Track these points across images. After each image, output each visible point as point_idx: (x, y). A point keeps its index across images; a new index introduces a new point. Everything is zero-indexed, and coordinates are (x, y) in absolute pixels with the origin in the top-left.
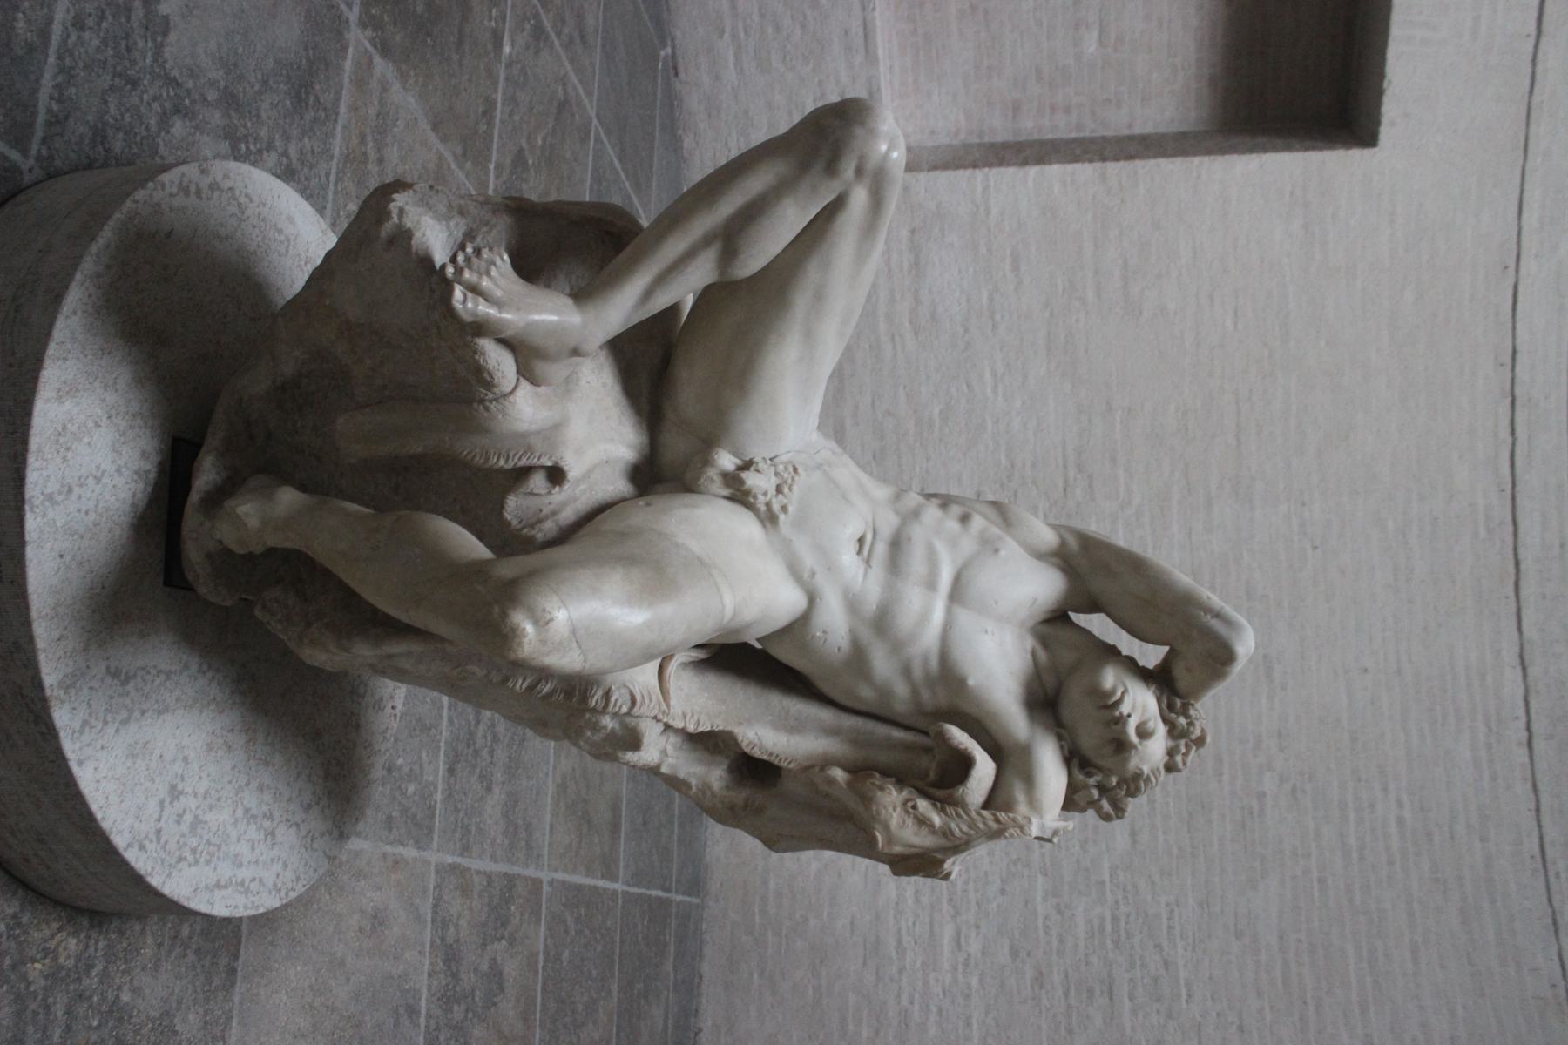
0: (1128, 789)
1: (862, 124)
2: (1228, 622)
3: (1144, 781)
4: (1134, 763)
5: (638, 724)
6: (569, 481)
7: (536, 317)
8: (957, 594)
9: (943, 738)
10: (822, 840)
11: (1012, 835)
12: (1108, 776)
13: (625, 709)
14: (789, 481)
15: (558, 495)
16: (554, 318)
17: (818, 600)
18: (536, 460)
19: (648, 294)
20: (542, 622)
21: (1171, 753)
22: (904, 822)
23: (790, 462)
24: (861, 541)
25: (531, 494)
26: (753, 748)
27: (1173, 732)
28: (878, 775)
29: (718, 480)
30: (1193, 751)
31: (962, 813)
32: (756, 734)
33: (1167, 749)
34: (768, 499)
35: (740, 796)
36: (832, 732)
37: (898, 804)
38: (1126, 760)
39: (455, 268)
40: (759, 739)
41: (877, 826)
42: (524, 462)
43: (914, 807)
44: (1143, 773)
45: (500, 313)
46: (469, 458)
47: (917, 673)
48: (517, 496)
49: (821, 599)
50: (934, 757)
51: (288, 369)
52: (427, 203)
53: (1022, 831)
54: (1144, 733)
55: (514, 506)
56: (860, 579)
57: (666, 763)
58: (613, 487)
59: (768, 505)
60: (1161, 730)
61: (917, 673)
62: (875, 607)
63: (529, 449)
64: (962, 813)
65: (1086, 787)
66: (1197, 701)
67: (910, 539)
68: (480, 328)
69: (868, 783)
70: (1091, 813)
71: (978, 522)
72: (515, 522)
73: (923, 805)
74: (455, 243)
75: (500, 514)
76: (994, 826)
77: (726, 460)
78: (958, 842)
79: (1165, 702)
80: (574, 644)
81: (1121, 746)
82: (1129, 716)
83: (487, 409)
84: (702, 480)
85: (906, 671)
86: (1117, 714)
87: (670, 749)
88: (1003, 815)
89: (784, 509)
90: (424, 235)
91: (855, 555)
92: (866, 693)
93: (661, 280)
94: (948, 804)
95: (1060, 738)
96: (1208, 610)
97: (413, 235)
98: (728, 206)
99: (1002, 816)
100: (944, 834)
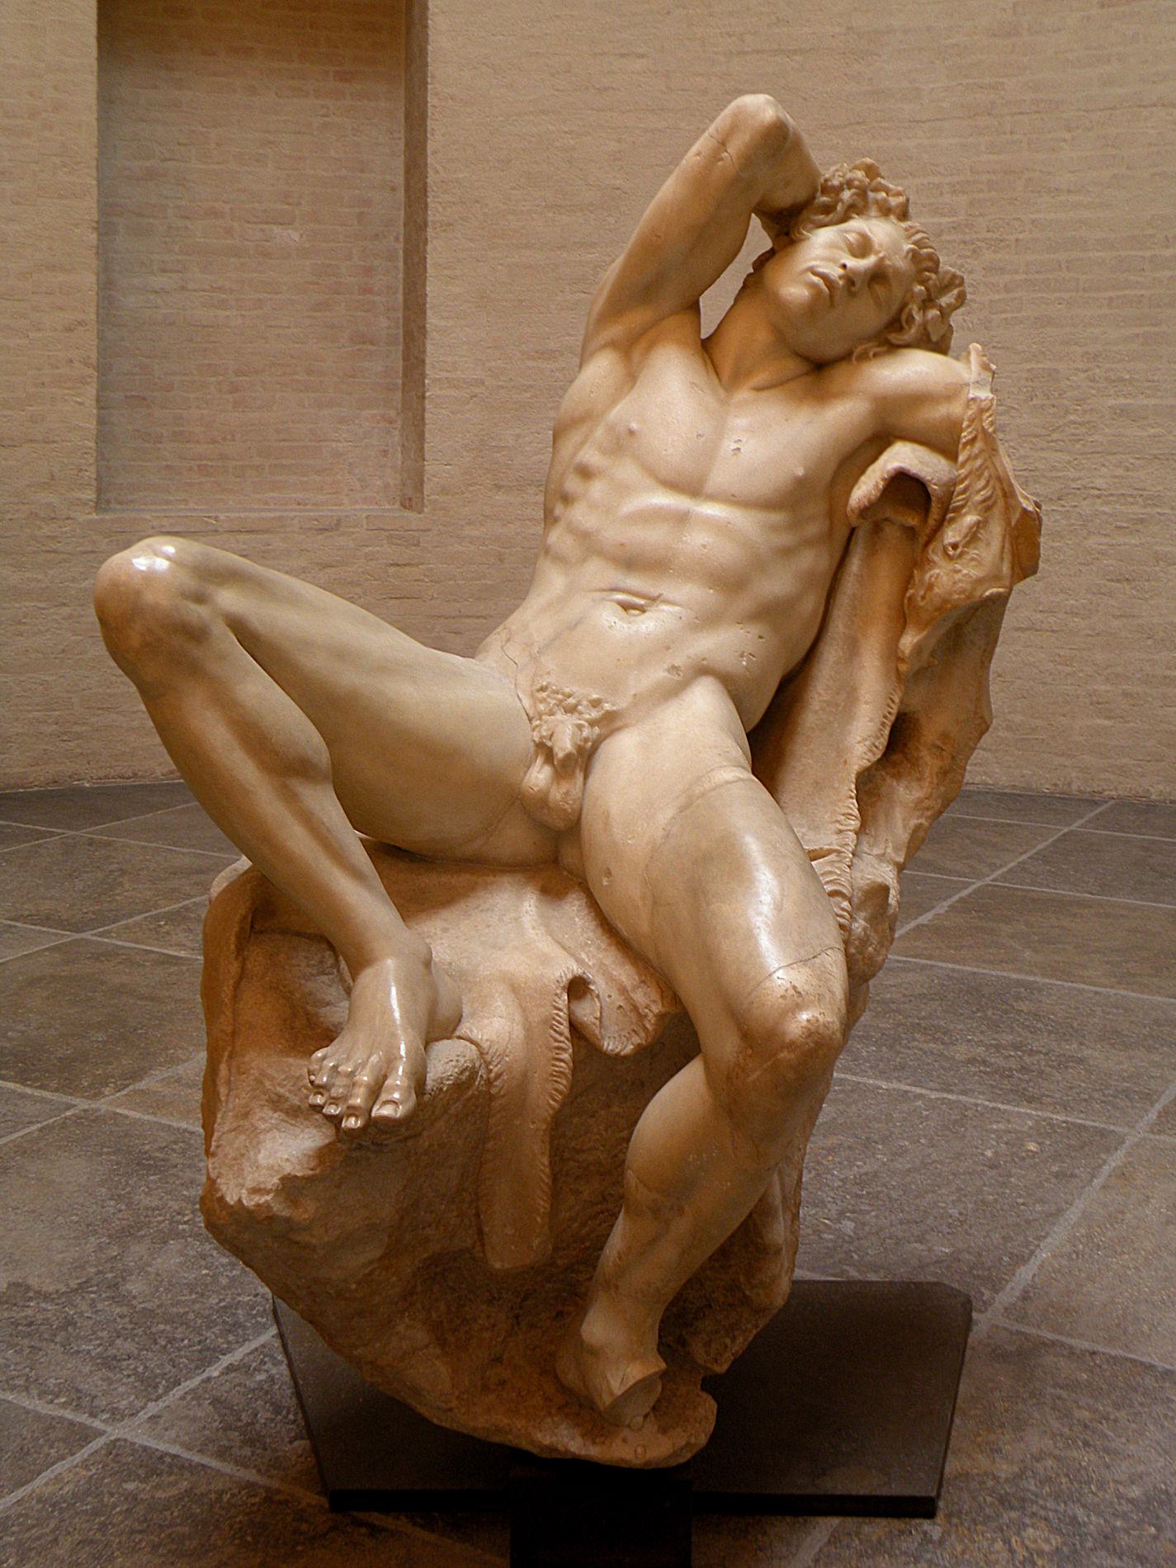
0: (928, 271)
1: (138, 593)
2: (733, 128)
3: (921, 248)
4: (900, 263)
5: (860, 889)
6: (584, 973)
7: (397, 1015)
8: (693, 488)
9: (865, 511)
10: (983, 663)
11: (992, 423)
13: (845, 904)
14: (560, 697)
15: (599, 985)
16: (394, 991)
17: (704, 662)
18: (561, 1014)
19: (356, 874)
20: (798, 1000)
21: (885, 211)
22: (973, 559)
23: (532, 696)
24: (626, 607)
25: (600, 1019)
26: (876, 747)
27: (856, 209)
28: (911, 591)
29: (564, 787)
30: (883, 181)
31: (962, 486)
32: (859, 742)
34: (586, 724)
35: (930, 763)
36: (853, 649)
37: (950, 566)
38: (897, 272)
39: (349, 1116)
40: (865, 740)
41: (978, 593)
42: (564, 1028)
43: (955, 546)
44: (912, 250)
45: (401, 1057)
46: (559, 1097)
47: (785, 539)
48: (603, 1038)
49: (703, 660)
50: (886, 520)
51: (421, 1336)
52: (235, 1159)
53: (988, 410)
54: (863, 247)
55: (617, 1042)
56: (677, 608)
57: (893, 855)
58: (577, 919)
59: (592, 723)
60: (856, 224)
61: (785, 539)
62: (711, 591)
63: (548, 1022)
64: (962, 486)
65: (925, 325)
66: (819, 175)
67: (622, 545)
68: (418, 1083)
69: (922, 604)
70: (956, 319)
71: (590, 456)
72: (637, 1040)
73: (951, 535)
74: (287, 1122)
75: (625, 1057)
76: (979, 445)
77: (539, 776)
78: (999, 493)
79: (822, 217)
80: (817, 961)
81: (878, 276)
82: (844, 266)
83: (498, 1076)
84: (567, 806)
85: (787, 552)
86: (841, 282)
87: (876, 851)
88: (963, 435)
89: (596, 704)
90: (287, 1160)
91: (647, 614)
92: (811, 604)
93: (338, 856)
94: (949, 504)
95: (864, 357)
96: (715, 156)
97: (289, 1174)
98: (244, 769)
99: (966, 436)
100: (988, 509)
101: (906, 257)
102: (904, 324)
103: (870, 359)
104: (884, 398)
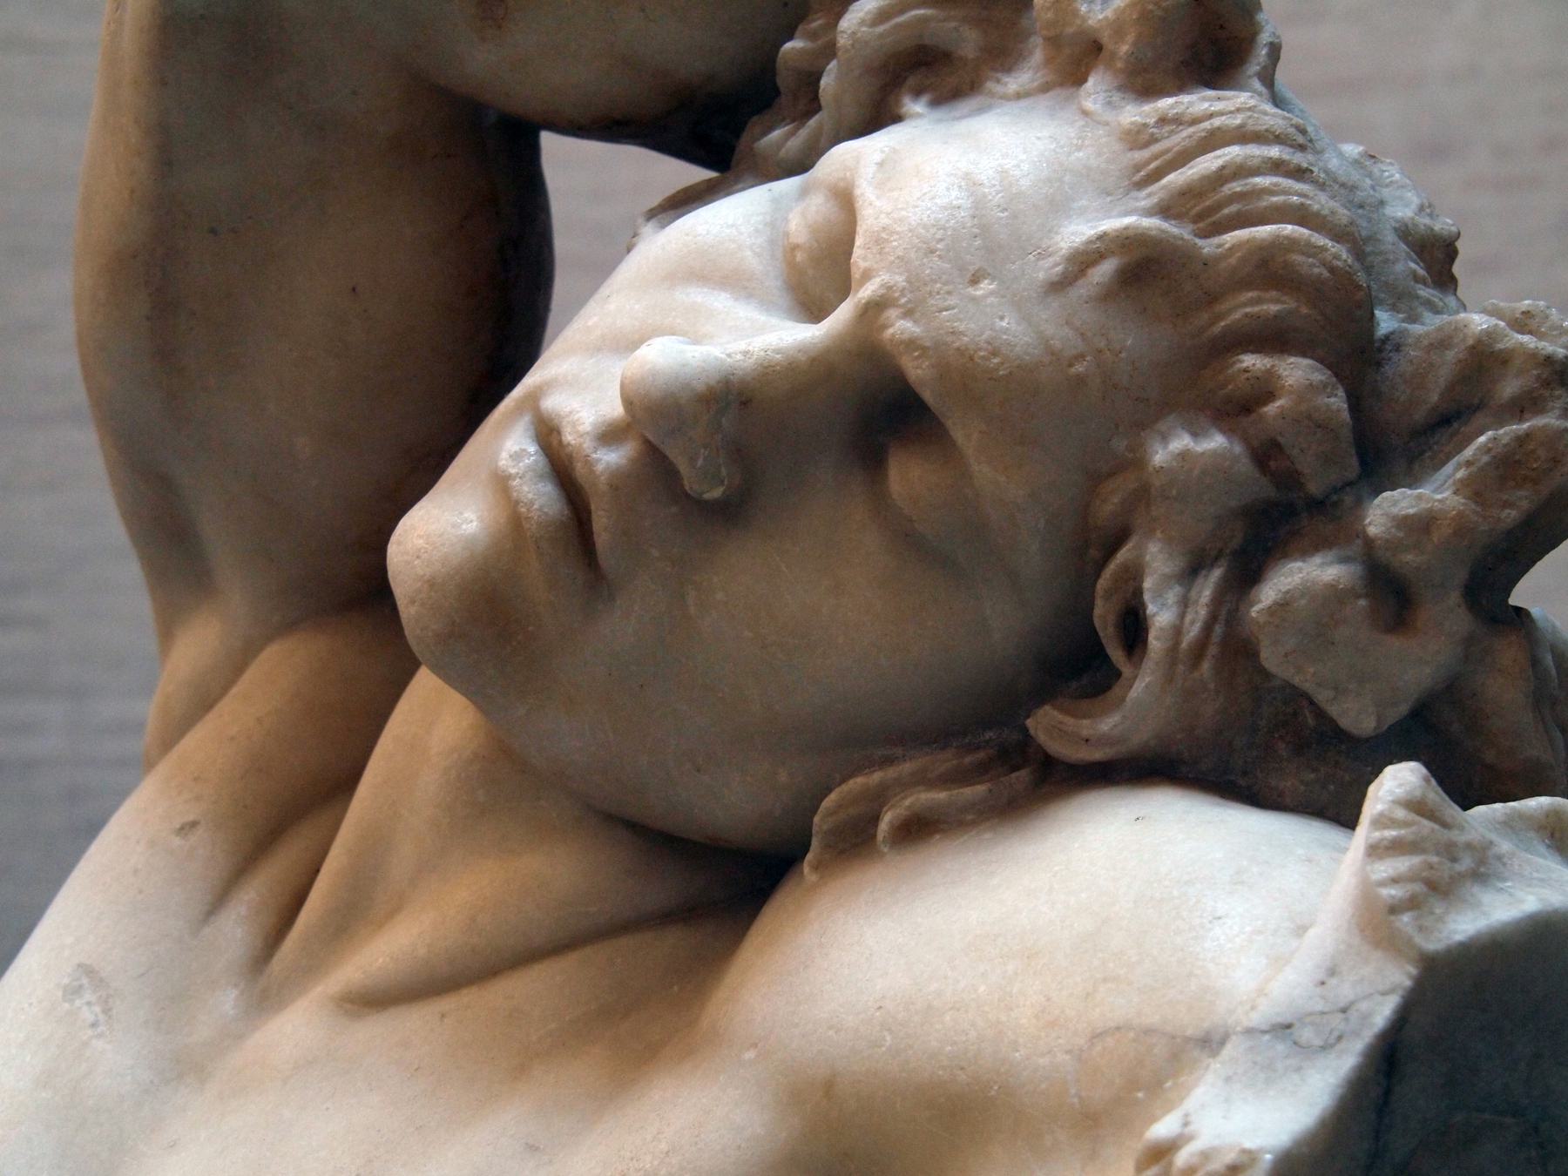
0: (1274, 339)
12: (1142, 495)
33: (1045, 88)
86: (610, 459)
101: (1059, 285)
102: (1116, 654)
103: (882, 855)
104: (829, 1086)
